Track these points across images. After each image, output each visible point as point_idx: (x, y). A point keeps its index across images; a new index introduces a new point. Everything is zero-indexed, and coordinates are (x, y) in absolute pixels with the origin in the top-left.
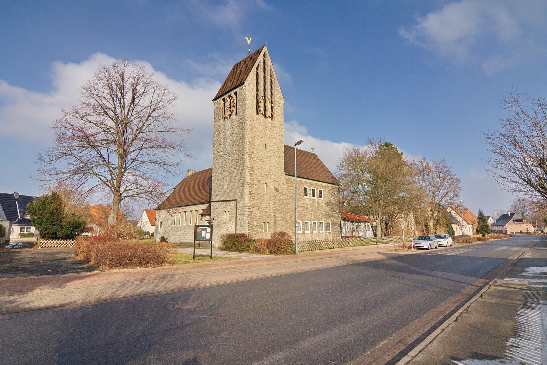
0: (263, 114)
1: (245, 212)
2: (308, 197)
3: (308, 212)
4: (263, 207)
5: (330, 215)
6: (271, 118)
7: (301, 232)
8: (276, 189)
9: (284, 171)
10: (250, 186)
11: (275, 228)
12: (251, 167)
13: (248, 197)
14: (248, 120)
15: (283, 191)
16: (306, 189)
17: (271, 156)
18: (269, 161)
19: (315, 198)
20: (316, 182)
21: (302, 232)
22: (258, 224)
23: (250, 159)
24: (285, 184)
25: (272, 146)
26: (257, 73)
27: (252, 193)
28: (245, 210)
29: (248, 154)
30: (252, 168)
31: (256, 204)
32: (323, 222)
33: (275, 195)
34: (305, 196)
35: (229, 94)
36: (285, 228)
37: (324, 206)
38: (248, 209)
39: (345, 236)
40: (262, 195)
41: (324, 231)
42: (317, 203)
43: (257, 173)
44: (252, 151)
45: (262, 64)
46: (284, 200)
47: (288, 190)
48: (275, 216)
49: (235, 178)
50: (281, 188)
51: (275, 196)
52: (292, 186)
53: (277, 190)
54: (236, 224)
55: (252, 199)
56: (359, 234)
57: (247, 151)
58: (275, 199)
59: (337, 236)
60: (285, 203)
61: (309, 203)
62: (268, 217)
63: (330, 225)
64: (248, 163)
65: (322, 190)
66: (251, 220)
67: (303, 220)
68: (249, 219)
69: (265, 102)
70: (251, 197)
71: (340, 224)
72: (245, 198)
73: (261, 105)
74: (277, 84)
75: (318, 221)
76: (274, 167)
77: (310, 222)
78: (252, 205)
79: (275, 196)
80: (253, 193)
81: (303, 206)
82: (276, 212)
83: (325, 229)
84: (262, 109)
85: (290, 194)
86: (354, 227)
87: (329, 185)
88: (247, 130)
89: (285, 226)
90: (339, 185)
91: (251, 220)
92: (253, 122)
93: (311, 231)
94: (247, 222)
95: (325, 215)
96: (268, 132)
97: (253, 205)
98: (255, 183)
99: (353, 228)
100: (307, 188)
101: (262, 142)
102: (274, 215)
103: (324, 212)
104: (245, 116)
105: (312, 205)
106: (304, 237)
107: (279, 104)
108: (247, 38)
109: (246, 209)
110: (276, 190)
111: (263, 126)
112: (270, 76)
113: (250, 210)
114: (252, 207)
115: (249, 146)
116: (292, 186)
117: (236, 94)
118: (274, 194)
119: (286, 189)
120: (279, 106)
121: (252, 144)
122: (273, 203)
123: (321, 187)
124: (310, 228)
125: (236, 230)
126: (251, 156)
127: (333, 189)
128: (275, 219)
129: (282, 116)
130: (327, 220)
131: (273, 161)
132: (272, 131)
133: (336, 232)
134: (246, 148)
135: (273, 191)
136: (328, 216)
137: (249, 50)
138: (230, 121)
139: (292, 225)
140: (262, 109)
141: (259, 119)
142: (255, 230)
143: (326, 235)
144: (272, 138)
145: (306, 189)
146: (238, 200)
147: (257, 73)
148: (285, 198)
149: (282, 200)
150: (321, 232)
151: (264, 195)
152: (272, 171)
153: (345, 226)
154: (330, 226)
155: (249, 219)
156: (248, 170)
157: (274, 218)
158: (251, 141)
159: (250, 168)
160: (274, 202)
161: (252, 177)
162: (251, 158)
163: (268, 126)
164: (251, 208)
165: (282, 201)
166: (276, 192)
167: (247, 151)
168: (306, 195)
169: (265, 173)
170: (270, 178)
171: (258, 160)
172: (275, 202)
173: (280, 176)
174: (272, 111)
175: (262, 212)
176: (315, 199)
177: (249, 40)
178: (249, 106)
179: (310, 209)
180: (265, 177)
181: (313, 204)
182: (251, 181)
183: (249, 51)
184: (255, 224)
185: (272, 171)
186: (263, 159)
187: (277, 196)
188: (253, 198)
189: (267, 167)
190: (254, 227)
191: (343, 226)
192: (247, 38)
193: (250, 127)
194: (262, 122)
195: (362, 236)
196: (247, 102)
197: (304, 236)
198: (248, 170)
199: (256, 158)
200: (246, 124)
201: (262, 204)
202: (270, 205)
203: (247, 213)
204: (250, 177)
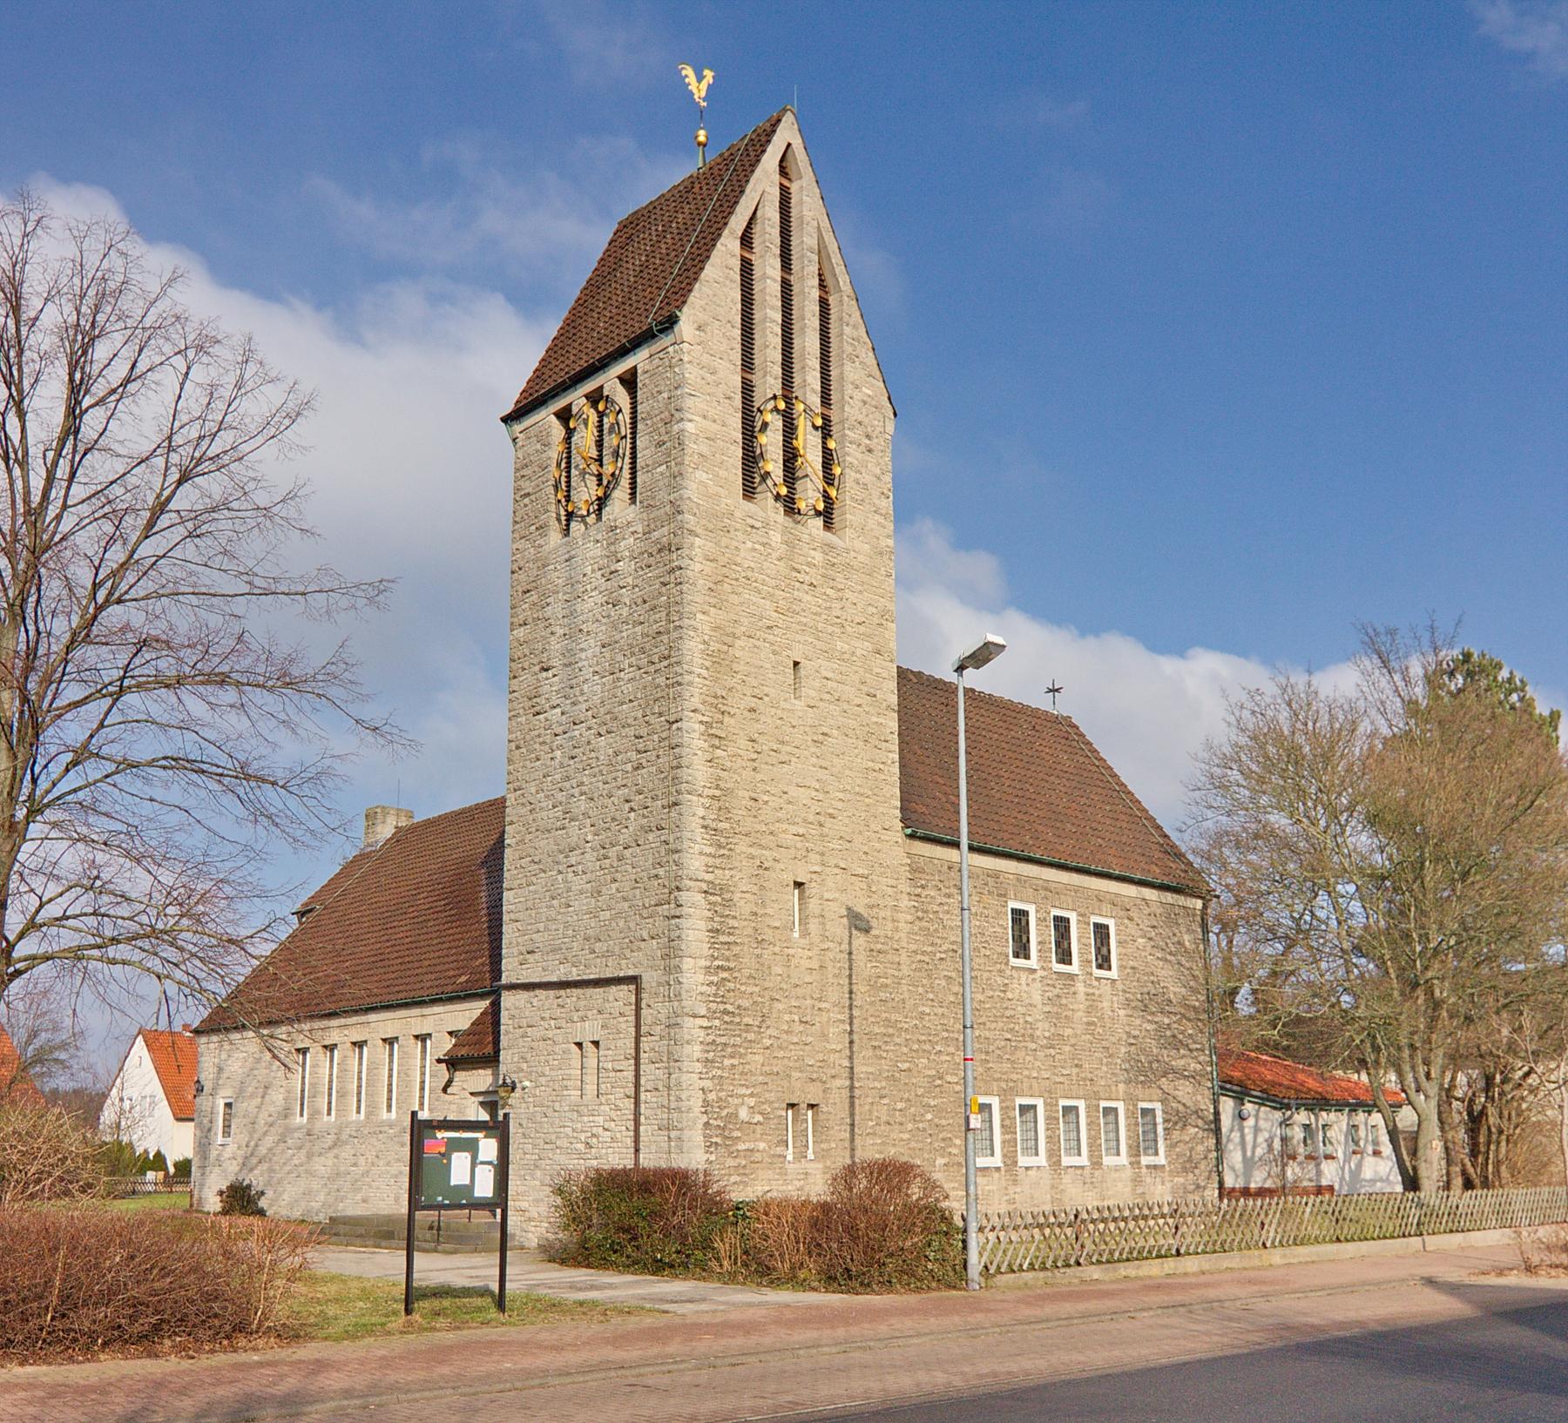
0: (777, 497)
1: (687, 1049)
2: (1033, 962)
3: (1034, 1046)
4: (787, 1017)
5: (1155, 1065)
6: (827, 515)
7: (997, 1160)
9: (898, 813)
10: (712, 898)
11: (852, 1140)
12: (717, 793)
13: (703, 963)
14: (699, 531)
15: (897, 929)
16: (1020, 917)
17: (825, 730)
18: (814, 760)
19: (1075, 968)
20: (1076, 879)
22: (759, 1118)
23: (713, 746)
24: (905, 887)
25: (830, 675)
26: (746, 268)
27: (723, 938)
28: (687, 1037)
29: (701, 718)
30: (721, 798)
31: (745, 1003)
32: (1120, 1106)
34: (1016, 955)
35: (590, 386)
36: (906, 1136)
37: (1122, 1012)
38: (702, 1033)
39: (1240, 1184)
40: (777, 949)
41: (1124, 1159)
42: (1081, 997)
43: (749, 824)
44: (718, 704)
45: (771, 213)
48: (852, 1068)
49: (627, 853)
50: (882, 914)
51: (850, 960)
52: (945, 900)
53: (863, 925)
54: (637, 1114)
55: (725, 975)
56: (1319, 1173)
58: (850, 976)
59: (1198, 1187)
60: (906, 995)
61: (1037, 998)
62: (814, 1076)
63: (1159, 1120)
64: (698, 772)
65: (1111, 923)
66: (723, 1094)
67: (1006, 1094)
68: (708, 1084)
69: (790, 430)
70: (717, 963)
71: (1212, 1117)
72: (685, 967)
73: (771, 441)
74: (855, 327)
75: (1092, 1098)
76: (841, 795)
78: (722, 1007)
79: (850, 960)
81: (1008, 1013)
83: (1130, 1147)
84: (774, 465)
86: (1289, 1133)
87: (1150, 894)
88: (694, 584)
89: (910, 1126)
90: (1206, 896)
91: (723, 1094)
92: (724, 541)
95: (1127, 1066)
97: (730, 1008)
98: (741, 880)
99: (1284, 1140)
100: (1025, 913)
101: (775, 653)
102: (846, 1063)
103: (1123, 1050)
104: (684, 508)
105: (1057, 1012)
106: (1011, 1190)
107: (868, 437)
108: (688, 72)
109: (692, 1028)
110: (858, 923)
111: (781, 563)
112: (816, 282)
113: (711, 1038)
114: (727, 1018)
115: (704, 673)
116: (945, 900)
117: (629, 382)
118: (845, 947)
119: (909, 918)
120: (870, 451)
121: (720, 661)
122: (837, 994)
123: (1106, 908)
124: (1047, 1137)
125: (637, 1150)
127: (1171, 917)
128: (852, 1088)
129: (887, 505)
130: (1139, 1091)
131: (836, 760)
132: (829, 591)
133: (1190, 1160)
134: (690, 684)
135: (839, 928)
136: (1145, 1072)
137: (702, 138)
138: (599, 537)
139: (944, 1122)
140: (774, 465)
141: (758, 525)
142: (741, 1146)
143: (1137, 1181)
144: (830, 629)
145: (1020, 917)
146: (650, 979)
147: (746, 268)
148: (905, 970)
149: (889, 981)
150: (1108, 1160)
151: (791, 951)
152: (832, 816)
153: (1241, 1129)
154: (1160, 1129)
155: (708, 1084)
156: (701, 812)
157: (848, 1083)
158: (715, 646)
159: (713, 797)
160: (846, 989)
161: (722, 852)
162: (717, 742)
163: (809, 564)
164: (717, 1022)
165: (887, 986)
167: (695, 702)
168: (1022, 950)
169: (794, 829)
170: (823, 854)
171: (755, 756)
172: (851, 992)
173: (878, 846)
174: (829, 478)
175: (780, 1047)
176: (1071, 977)
177: (700, 78)
179: (1043, 1029)
180: (792, 851)
181: (1064, 1001)
183: (699, 144)
184: (743, 1114)
185: (832, 816)
186: (785, 749)
187: (860, 958)
188: (729, 969)
190: (737, 1134)
191: (1232, 1131)
192: (688, 72)
193: (709, 567)
194: (776, 538)
195: (1337, 1187)
196: (689, 427)
197: (1015, 1182)
198: (701, 812)
199: (743, 742)
200: (685, 552)
202: (823, 1005)
203: (696, 1051)
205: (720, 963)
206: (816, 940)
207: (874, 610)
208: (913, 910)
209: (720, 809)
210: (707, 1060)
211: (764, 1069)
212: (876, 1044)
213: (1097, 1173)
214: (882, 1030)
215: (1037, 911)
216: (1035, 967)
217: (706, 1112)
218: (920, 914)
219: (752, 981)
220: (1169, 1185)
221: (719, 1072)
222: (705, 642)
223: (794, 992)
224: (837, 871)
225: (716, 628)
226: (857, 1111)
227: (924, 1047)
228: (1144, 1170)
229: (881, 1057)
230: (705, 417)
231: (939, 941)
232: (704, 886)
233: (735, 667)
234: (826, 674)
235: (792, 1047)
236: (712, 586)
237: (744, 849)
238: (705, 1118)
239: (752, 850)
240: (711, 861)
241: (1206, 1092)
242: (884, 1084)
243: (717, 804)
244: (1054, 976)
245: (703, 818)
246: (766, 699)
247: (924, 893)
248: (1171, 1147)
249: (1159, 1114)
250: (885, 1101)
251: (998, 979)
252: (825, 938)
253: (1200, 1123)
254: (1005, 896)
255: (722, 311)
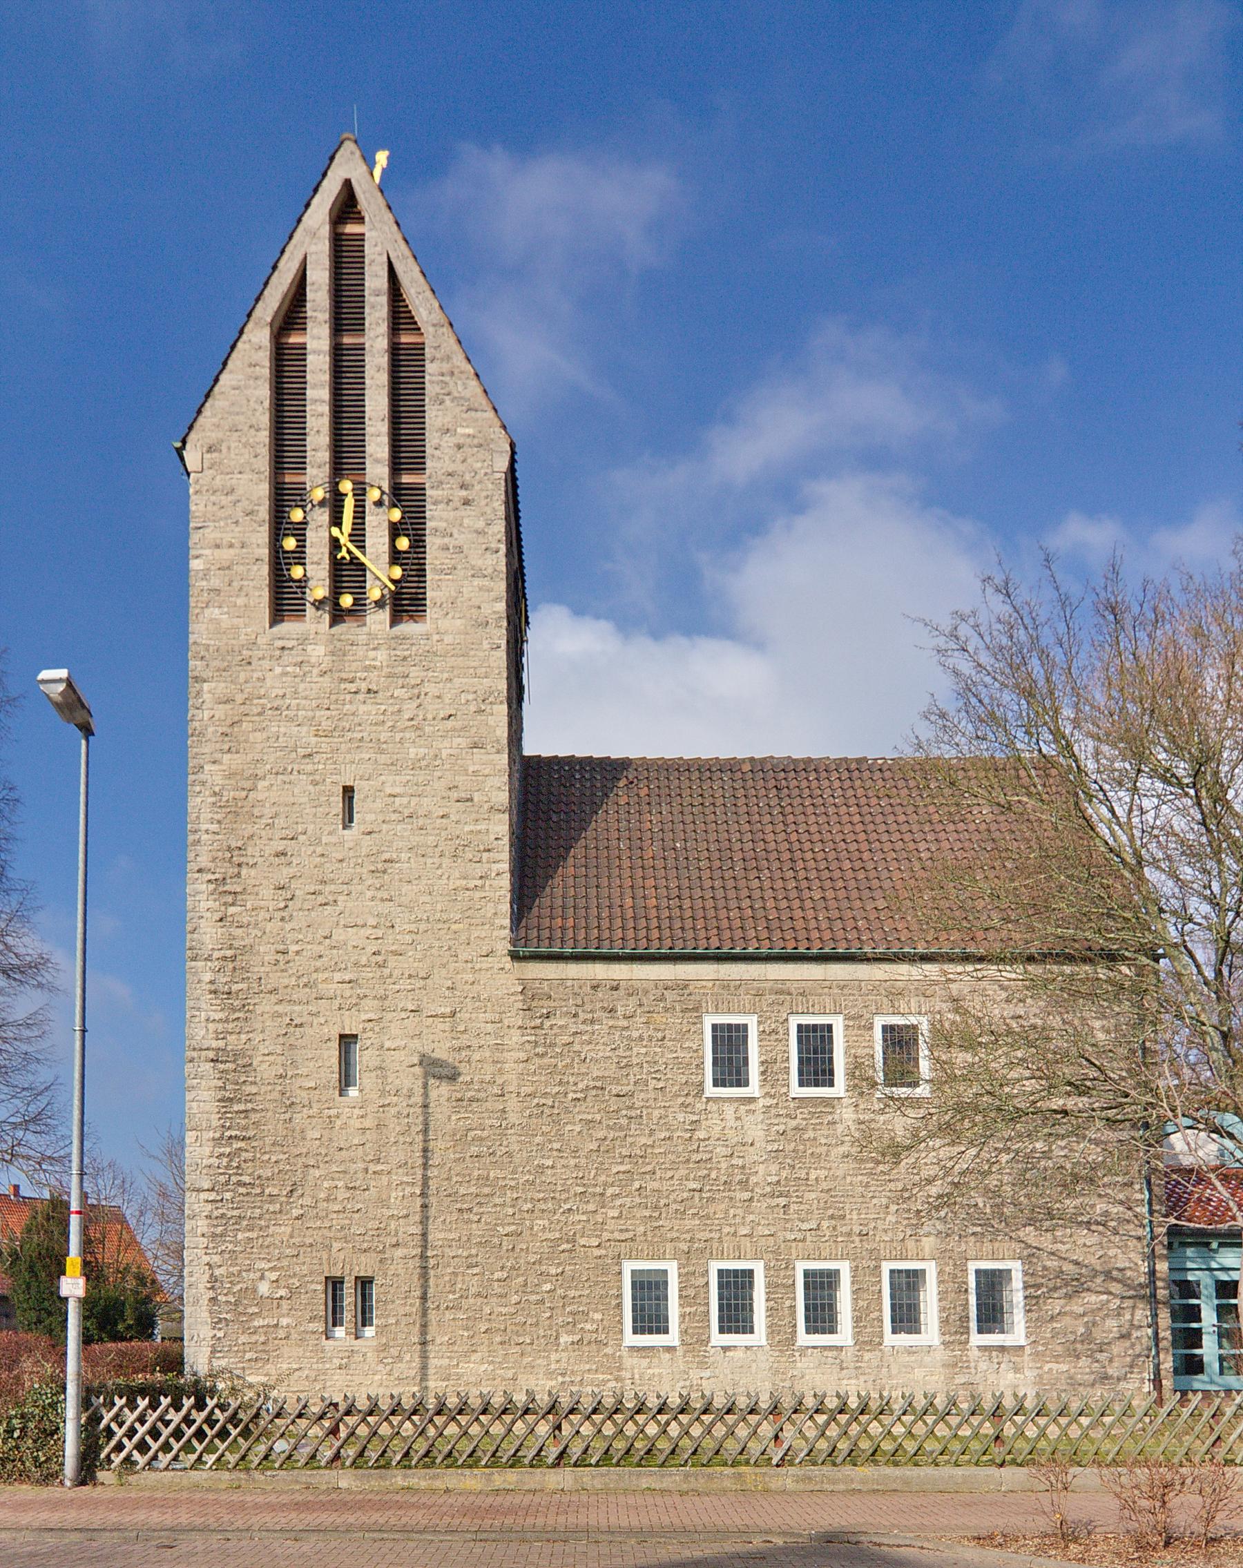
2: (754, 1088)
3: (747, 1195)
4: (326, 1184)
8: (436, 1063)
10: (221, 1066)
11: (424, 1313)
12: (229, 953)
13: (211, 1134)
17: (386, 856)
21: (676, 1343)
22: (282, 1292)
23: (225, 904)
25: (398, 790)
27: (236, 1108)
33: (426, 1106)
38: (209, 1207)
43: (275, 980)
44: (235, 856)
46: (502, 1131)
47: (546, 1061)
50: (476, 1056)
53: (445, 1072)
57: (204, 861)
58: (425, 1131)
59: (1106, 1377)
60: (516, 1147)
62: (365, 1245)
64: (207, 934)
66: (235, 1269)
67: (691, 1257)
68: (216, 1259)
70: (227, 1134)
77: (767, 1268)
79: (426, 1115)
80: (249, 1106)
82: (432, 1212)
83: (945, 1322)
85: (560, 1083)
89: (515, 1298)
93: (772, 1330)
94: (206, 1277)
96: (363, 708)
97: (246, 1179)
107: (463, 486)
109: (196, 1204)
111: (327, 678)
113: (216, 1213)
114: (242, 1190)
115: (214, 827)
118: (418, 1099)
119: (523, 1056)
122: (404, 1152)
124: (769, 1309)
126: (227, 888)
128: (423, 1257)
131: (406, 888)
133: (1087, 1338)
135: (410, 1080)
141: (289, 644)
143: (954, 1366)
144: (398, 736)
148: (513, 1118)
152: (395, 953)
155: (216, 1259)
159: (225, 958)
160: (418, 1147)
161: (237, 1015)
162: (230, 899)
163: (367, 669)
164: (228, 1195)
165: (482, 1139)
166: (432, 1081)
172: (425, 1150)
173: (470, 978)
176: (828, 1102)
178: (215, 582)
179: (765, 1174)
182: (232, 1038)
184: (264, 1288)
187: (440, 1113)
189: (354, 937)
193: (221, 710)
197: (703, 1365)
198: (207, 977)
201: (311, 1171)
202: (379, 1167)
203: (202, 1225)
204: (221, 1015)
205: (234, 1133)
206: (374, 1096)
207: (471, 697)
208: (528, 1046)
209: (234, 968)
210: (214, 1235)
211: (293, 1240)
212: (465, 1206)
213: (867, 1356)
214: (473, 1190)
215: (759, 1023)
216: (757, 1095)
217: (212, 1288)
218: (540, 1050)
219: (278, 1148)
220: (1030, 1374)
221: (231, 1247)
222: (215, 794)
223: (339, 1156)
224: (404, 1015)
225: (230, 776)
226: (432, 1282)
227: (543, 1207)
228: (976, 1353)
229: (471, 1222)
230: (218, 546)
231: (572, 1080)
232: (211, 1055)
233: (256, 812)
234: (389, 791)
235: (335, 1216)
236: (225, 729)
237: (267, 1008)
238: (211, 1294)
239: (277, 1008)
240: (220, 1027)
241: (1132, 1243)
242: (474, 1252)
243: (231, 966)
244: (792, 1105)
245: (212, 982)
246: (302, 838)
247: (547, 1024)
248: (1034, 1325)
249: (1017, 1281)
250: (476, 1270)
251: (681, 1117)
252: (383, 1093)
253: (1116, 1288)
254: (696, 1009)
255: (241, 418)
